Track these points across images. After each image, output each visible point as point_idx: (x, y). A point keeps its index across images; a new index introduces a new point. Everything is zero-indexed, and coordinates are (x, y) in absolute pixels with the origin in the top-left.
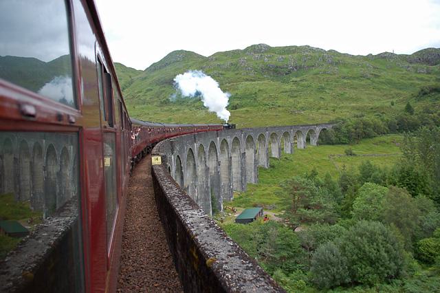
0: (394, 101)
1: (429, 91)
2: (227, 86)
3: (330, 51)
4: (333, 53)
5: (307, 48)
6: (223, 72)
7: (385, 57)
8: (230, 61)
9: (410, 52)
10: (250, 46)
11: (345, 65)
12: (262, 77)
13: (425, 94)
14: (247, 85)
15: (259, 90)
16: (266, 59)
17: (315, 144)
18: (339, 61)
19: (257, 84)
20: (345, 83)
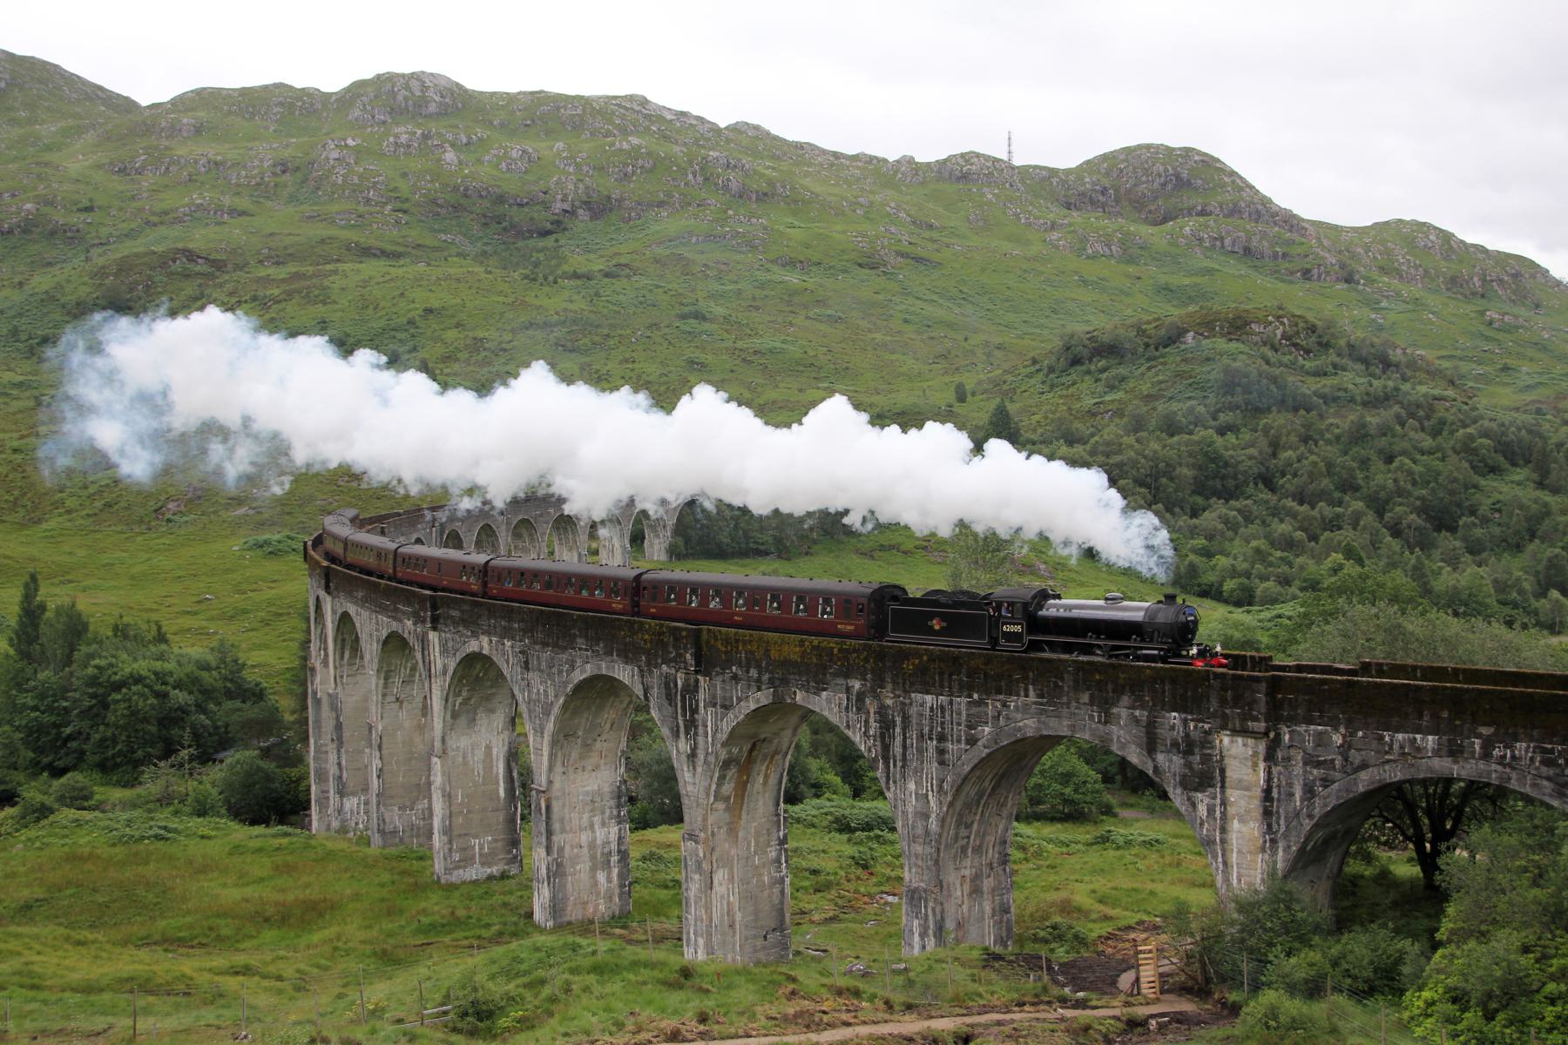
0: (970, 382)
1: (1086, 352)
2: (267, 281)
3: (737, 129)
4: (750, 139)
5: (632, 114)
6: (244, 203)
7: (964, 177)
8: (265, 153)
9: (1067, 159)
10: (368, 75)
11: (798, 203)
12: (429, 241)
13: (1076, 361)
14: (365, 284)
15: (429, 311)
16: (450, 156)
17: (663, 557)
18: (771, 183)
19: (418, 281)
20: (794, 293)
